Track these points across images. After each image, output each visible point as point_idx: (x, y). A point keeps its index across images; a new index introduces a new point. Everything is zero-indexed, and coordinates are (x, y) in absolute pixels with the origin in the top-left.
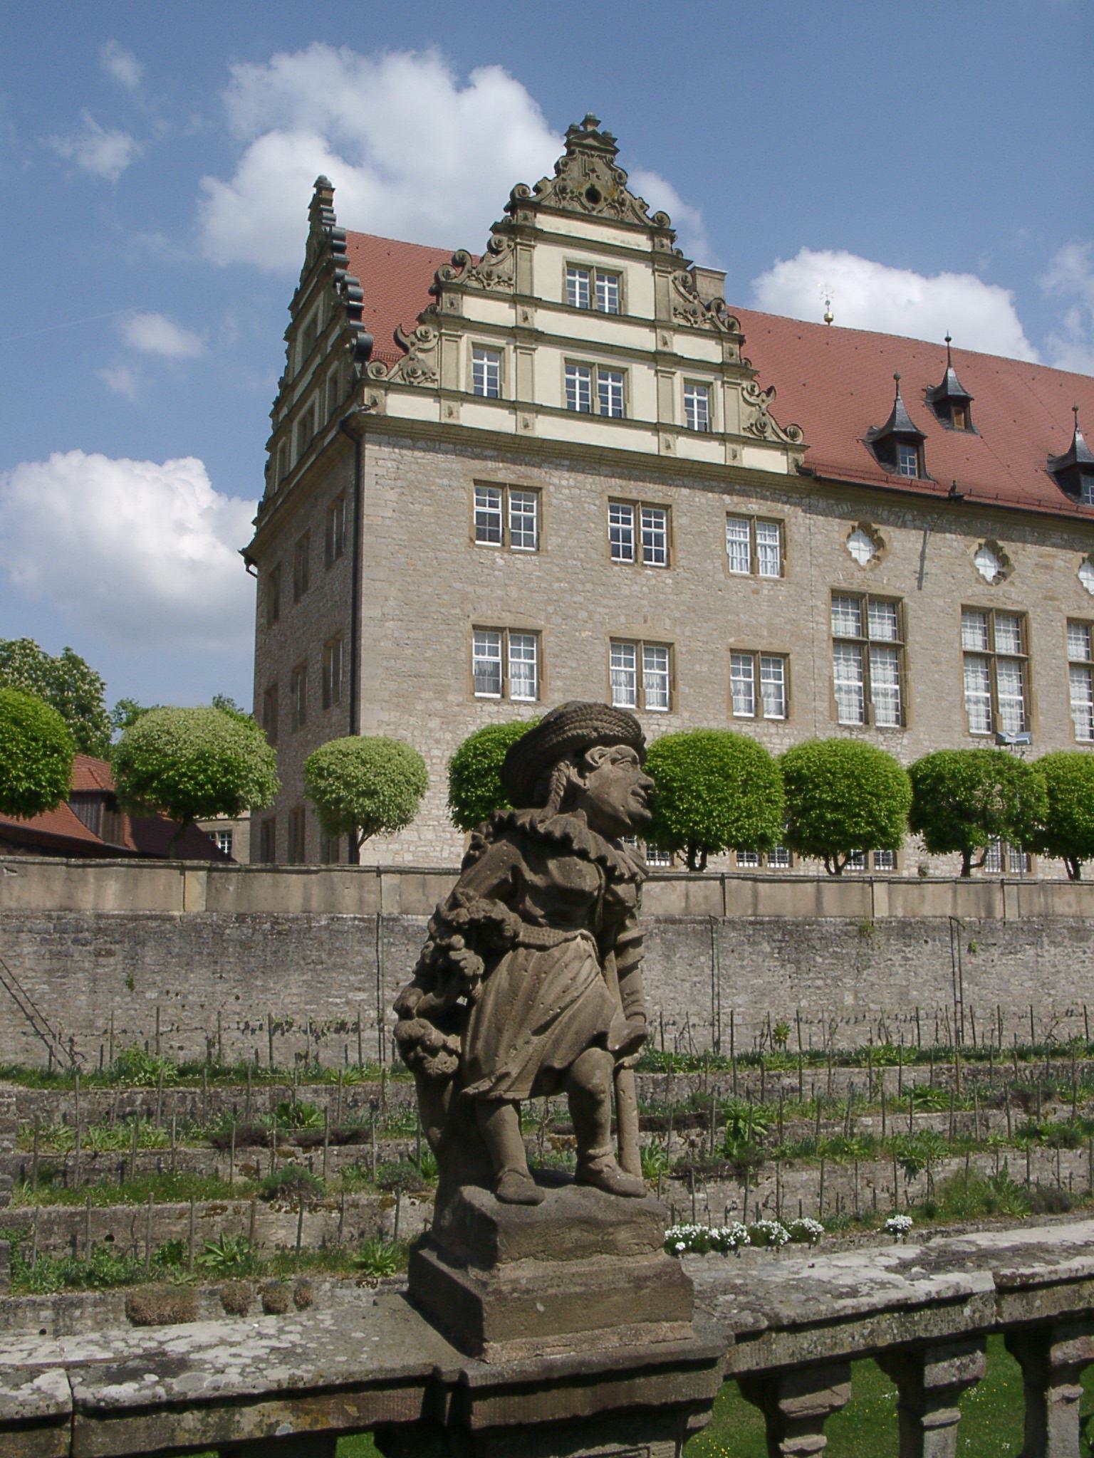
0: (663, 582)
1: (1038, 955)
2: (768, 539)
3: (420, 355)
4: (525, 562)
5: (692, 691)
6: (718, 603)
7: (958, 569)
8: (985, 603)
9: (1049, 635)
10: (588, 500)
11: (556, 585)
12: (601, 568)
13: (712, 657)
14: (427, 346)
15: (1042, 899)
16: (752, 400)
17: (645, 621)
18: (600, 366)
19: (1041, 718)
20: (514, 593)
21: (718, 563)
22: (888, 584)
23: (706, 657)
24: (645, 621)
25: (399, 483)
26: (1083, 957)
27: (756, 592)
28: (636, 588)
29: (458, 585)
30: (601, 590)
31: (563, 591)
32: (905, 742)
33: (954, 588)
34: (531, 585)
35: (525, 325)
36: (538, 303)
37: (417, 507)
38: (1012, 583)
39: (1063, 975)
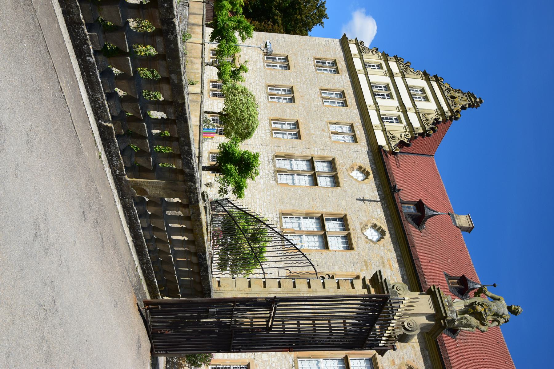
2: (348, 139)
3: (371, 53)
7: (364, 214)
8: (351, 227)
9: (345, 262)
14: (374, 53)
16: (403, 135)
18: (391, 93)
22: (344, 180)
23: (293, 113)
25: (328, 45)
27: (323, 130)
29: (300, 53)
31: (305, 76)
32: (271, 182)
33: (353, 211)
35: (394, 74)
36: (403, 77)
37: (321, 47)
38: (367, 242)
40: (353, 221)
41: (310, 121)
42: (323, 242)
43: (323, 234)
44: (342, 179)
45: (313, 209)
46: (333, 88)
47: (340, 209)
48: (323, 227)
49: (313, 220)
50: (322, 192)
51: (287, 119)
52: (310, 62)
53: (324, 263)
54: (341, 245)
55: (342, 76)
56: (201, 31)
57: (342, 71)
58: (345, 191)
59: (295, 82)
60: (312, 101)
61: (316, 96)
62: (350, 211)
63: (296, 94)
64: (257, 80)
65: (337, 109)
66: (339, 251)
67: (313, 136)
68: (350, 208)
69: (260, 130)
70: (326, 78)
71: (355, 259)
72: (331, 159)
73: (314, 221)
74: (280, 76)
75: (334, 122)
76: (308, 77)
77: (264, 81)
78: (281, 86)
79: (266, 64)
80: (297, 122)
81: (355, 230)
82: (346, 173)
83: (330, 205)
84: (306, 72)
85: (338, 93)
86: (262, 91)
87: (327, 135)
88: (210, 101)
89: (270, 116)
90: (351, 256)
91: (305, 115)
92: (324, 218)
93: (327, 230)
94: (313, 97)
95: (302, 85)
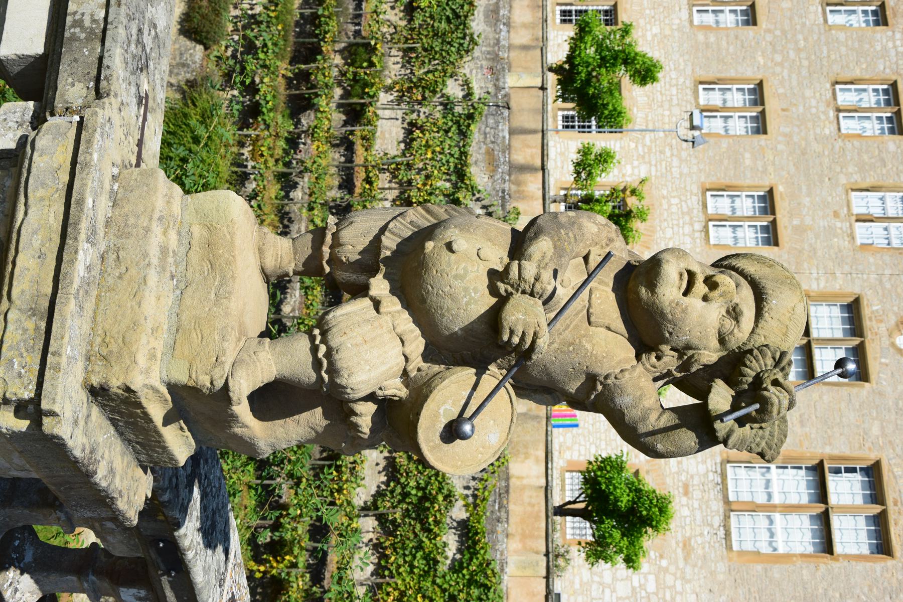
0: (824, 127)
4: (816, 13)
5: (724, 150)
6: (816, 177)
8: (890, 495)
9: (871, 590)
10: (888, 63)
11: (800, 37)
12: (825, 74)
13: (760, 169)
17: (783, 110)
19: (759, 567)
21: (857, 177)
22: (881, 363)
23: (760, 164)
24: (783, 110)
27: (836, 214)
28: (814, 102)
30: (804, 72)
31: (796, 42)
34: (796, 18)
40: (895, 477)
41: (804, 188)
42: (821, 531)
43: (823, 513)
44: (875, 359)
45: (801, 446)
46: (867, 77)
47: (867, 446)
48: (822, 494)
49: (800, 471)
50: (825, 397)
51: (746, 185)
53: (820, 591)
54: (863, 537)
55: (893, 32)
56: (539, 189)
57: (895, 15)
58: (881, 394)
59: (769, 63)
60: (810, 125)
61: (822, 108)
62: (891, 451)
63: (772, 105)
64: (672, 67)
65: (876, 145)
66: (859, 558)
67: (809, 232)
68: (890, 442)
69: (678, 225)
70: (850, 43)
71: (894, 581)
72: (852, 299)
73: (803, 472)
74: (731, 49)
75: (864, 186)
76: (802, 44)
77: (689, 71)
78: (733, 81)
79: (695, 9)
80: (771, 192)
81: (899, 504)
82: (886, 342)
83: (841, 434)
84: (798, 27)
85: (881, 87)
86: (684, 103)
87: (844, 229)
88: (558, 146)
89: (703, 179)
90: (885, 574)
91: (793, 170)
92: (827, 466)
93: (833, 499)
94: (814, 111)
95: (786, 72)
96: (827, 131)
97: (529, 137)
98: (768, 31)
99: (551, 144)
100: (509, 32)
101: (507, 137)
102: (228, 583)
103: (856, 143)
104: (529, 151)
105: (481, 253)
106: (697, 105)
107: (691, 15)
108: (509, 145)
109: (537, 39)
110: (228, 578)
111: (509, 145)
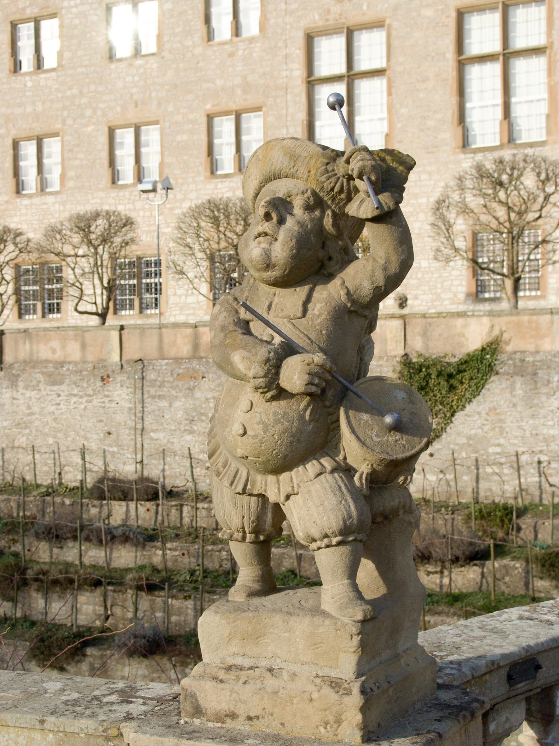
1: (14, 399)
4: (46, 79)
11: (69, 93)
13: (191, 126)
15: (28, 346)
20: (39, 108)
24: (136, 106)
26: (58, 400)
27: (231, 55)
30: (101, 89)
39: (37, 416)
52: (29, 84)
55: (62, 8)
59: (94, 120)
74: (81, 156)
77: (102, 194)
86: (133, 197)
88: (174, 313)
89: (202, 178)
94: (136, 78)
95: (102, 105)
96: (155, 66)
97: (166, 340)
98: (64, 122)
99: (172, 320)
100: (69, 363)
101: (166, 361)
102: (549, 617)
103: (166, 38)
104: (180, 341)
105: (241, 431)
106: (134, 185)
107: (51, 193)
108: (173, 359)
109: (76, 335)
110: (546, 617)
111: (173, 359)
